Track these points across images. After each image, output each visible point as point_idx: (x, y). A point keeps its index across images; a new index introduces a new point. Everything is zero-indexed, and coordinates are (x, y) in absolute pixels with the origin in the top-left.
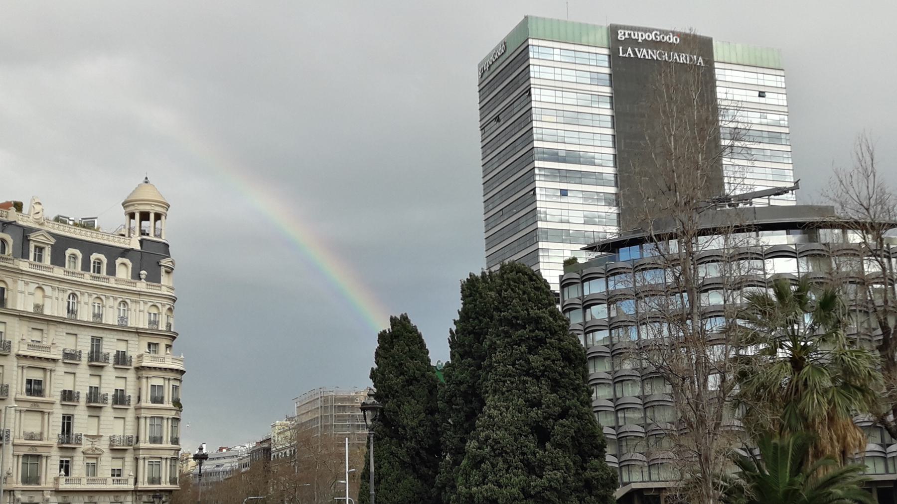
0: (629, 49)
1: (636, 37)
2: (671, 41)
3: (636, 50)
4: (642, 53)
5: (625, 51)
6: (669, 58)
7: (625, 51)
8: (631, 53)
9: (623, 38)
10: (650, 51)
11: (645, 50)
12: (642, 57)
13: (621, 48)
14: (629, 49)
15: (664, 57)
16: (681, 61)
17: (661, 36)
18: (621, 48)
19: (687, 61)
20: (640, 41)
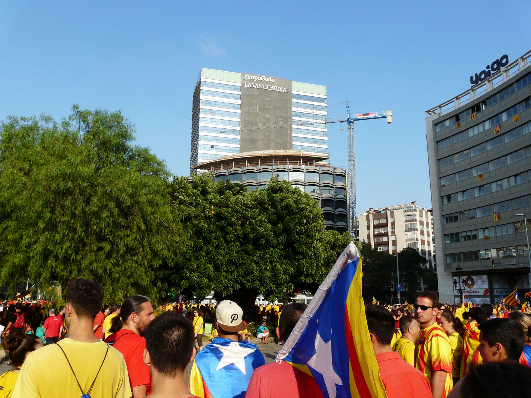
0: (250, 84)
1: (253, 79)
2: (271, 81)
3: (253, 84)
4: (256, 85)
5: (247, 84)
6: (269, 88)
7: (247, 84)
8: (250, 85)
9: (247, 79)
10: (259, 85)
11: (257, 84)
12: (255, 87)
13: (245, 83)
14: (250, 84)
15: (266, 87)
16: (275, 90)
17: (266, 78)
18: (245, 83)
19: (277, 89)
20: (255, 80)
